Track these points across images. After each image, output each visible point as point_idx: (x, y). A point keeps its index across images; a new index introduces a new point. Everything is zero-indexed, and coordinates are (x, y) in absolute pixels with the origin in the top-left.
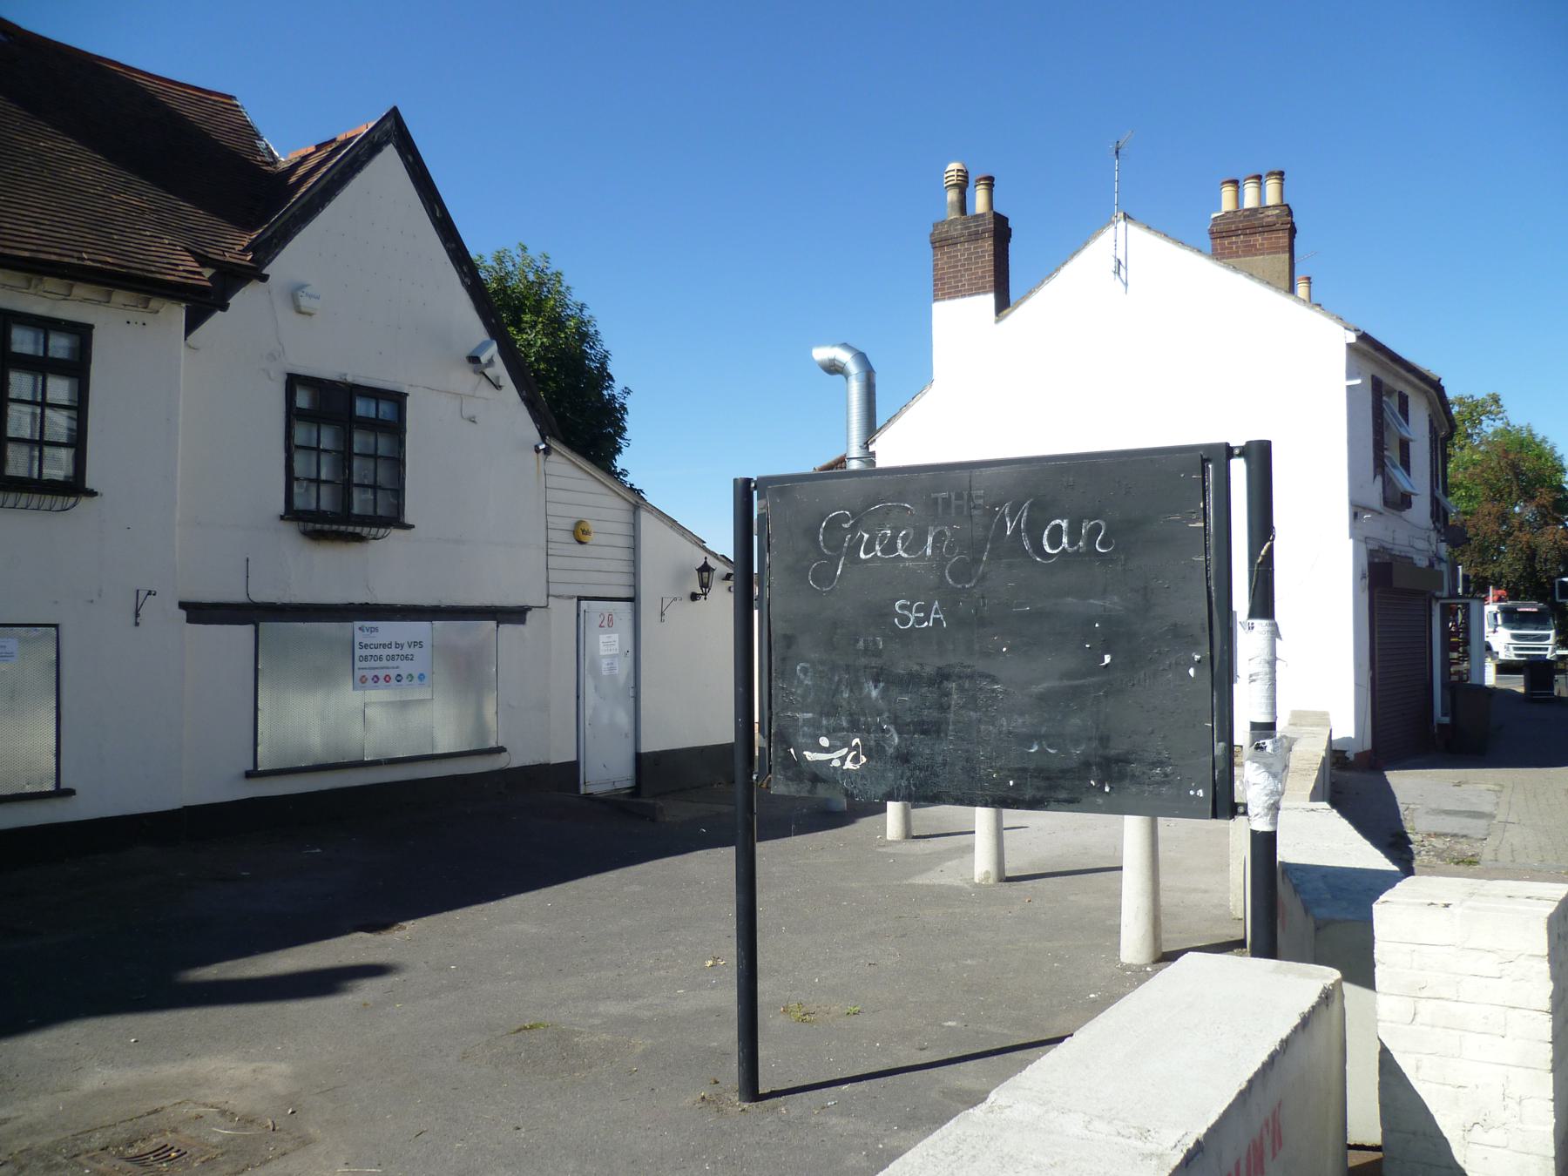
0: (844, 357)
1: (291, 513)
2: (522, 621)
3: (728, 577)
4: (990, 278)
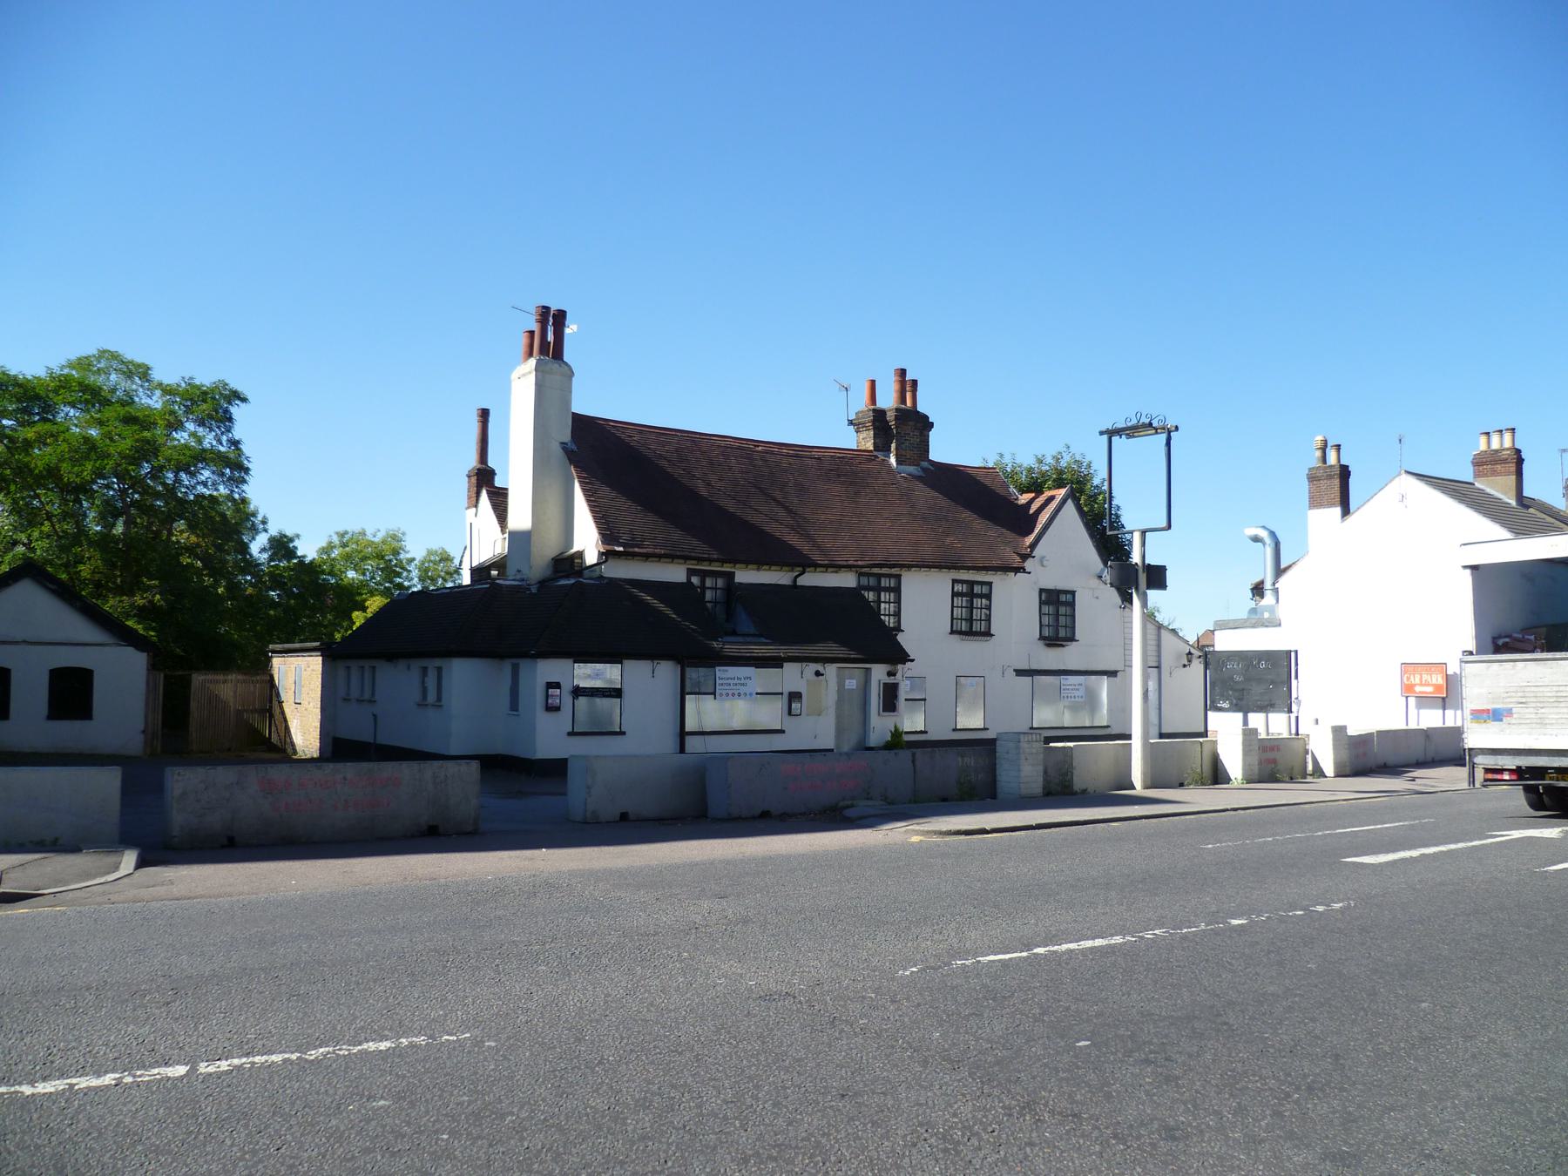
0: (1264, 534)
1: (1042, 638)
2: (1116, 676)
3: (1200, 657)
4: (1338, 499)
